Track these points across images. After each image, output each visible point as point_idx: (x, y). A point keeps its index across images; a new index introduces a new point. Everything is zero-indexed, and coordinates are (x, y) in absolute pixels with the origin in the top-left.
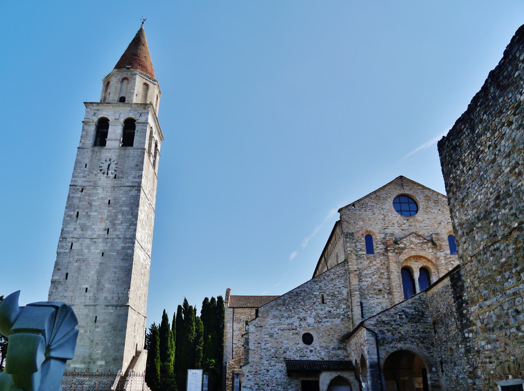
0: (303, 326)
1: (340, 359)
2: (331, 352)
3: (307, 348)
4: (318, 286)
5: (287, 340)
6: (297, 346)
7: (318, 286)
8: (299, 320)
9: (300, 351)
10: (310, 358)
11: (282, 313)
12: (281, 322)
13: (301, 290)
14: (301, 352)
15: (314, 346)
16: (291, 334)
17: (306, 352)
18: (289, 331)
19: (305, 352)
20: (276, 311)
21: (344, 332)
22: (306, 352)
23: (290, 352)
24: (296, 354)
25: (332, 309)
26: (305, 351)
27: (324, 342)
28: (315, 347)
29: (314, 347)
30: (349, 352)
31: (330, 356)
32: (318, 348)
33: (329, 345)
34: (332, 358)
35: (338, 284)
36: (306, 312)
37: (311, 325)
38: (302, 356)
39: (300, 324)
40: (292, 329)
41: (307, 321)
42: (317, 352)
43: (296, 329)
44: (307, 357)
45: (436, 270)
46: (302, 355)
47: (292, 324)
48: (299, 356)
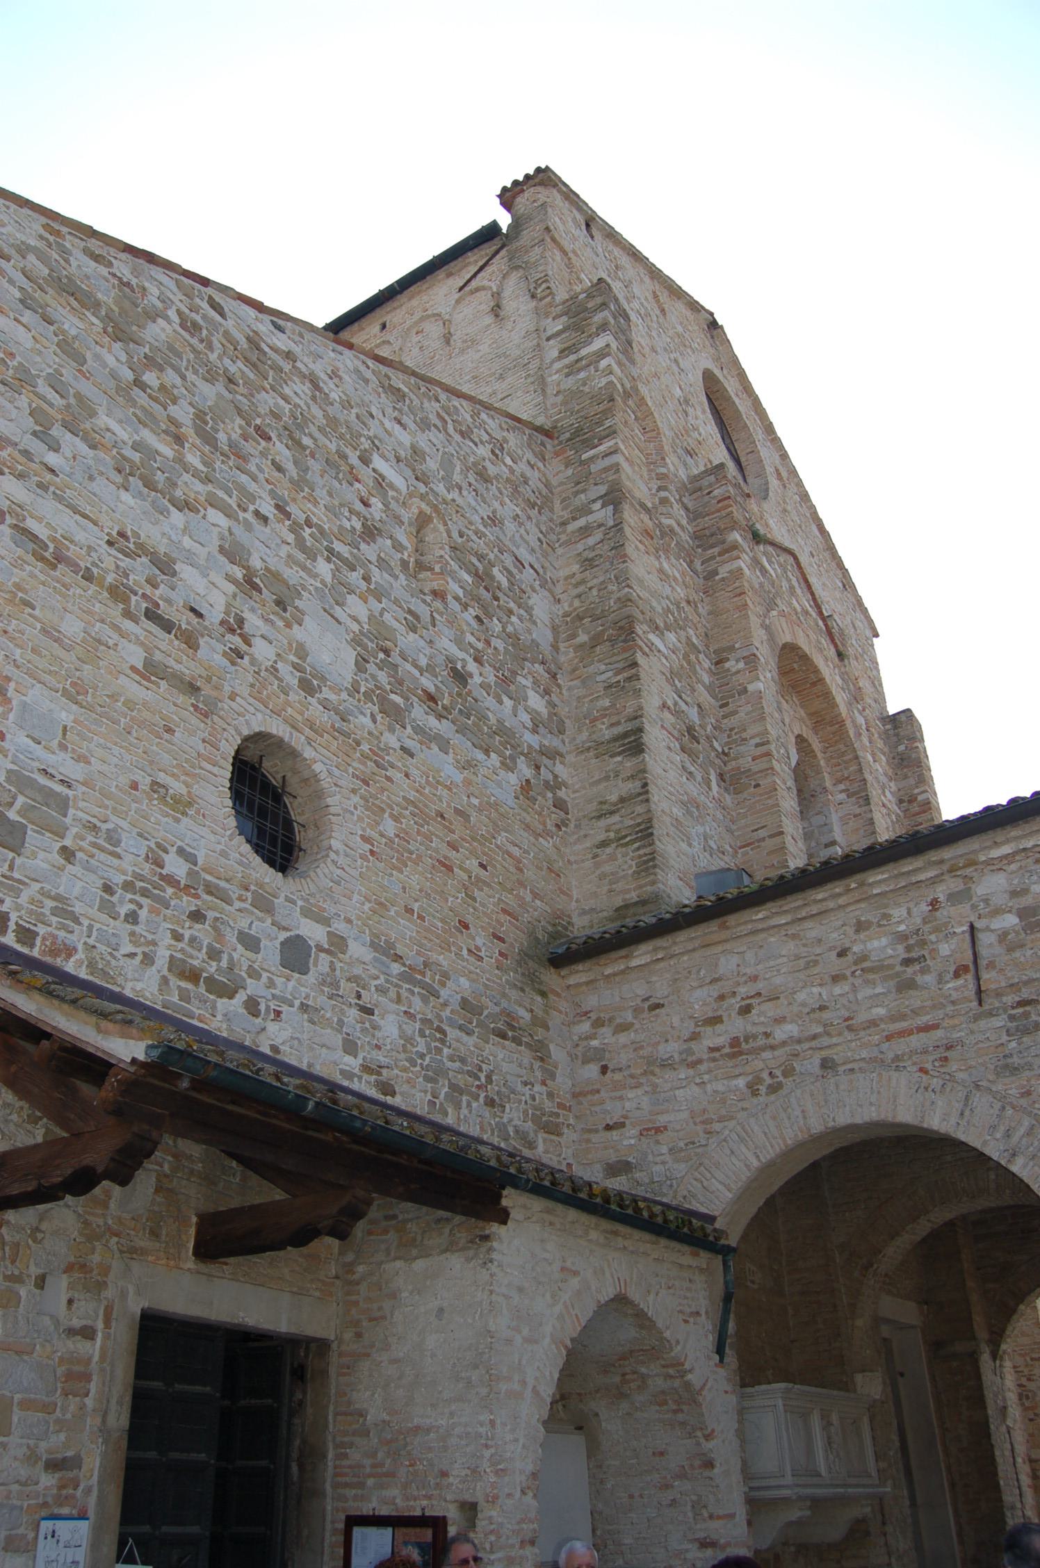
0: (263, 651)
1: (502, 1128)
2: (452, 1033)
3: (264, 904)
4: (405, 438)
5: (75, 693)
6: (162, 825)
7: (405, 438)
8: (239, 573)
9: (188, 903)
10: (272, 1027)
11: (85, 388)
12: (52, 459)
13: (289, 355)
14: (197, 916)
15: (331, 909)
16: (136, 657)
17: (251, 943)
18: (116, 611)
19: (232, 938)
20: (28, 317)
21: (536, 896)
22: (251, 943)
23: (68, 854)
24: (132, 918)
25: (472, 667)
26: (243, 924)
27: (409, 911)
28: (339, 927)
29: (325, 922)
30: (563, 1083)
31: (440, 1072)
32: (358, 950)
33: (444, 960)
34: (458, 1106)
35: (510, 526)
36: (301, 544)
37: (326, 693)
38: (193, 976)
39: (241, 621)
40: (151, 615)
41: (297, 631)
42: (346, 988)
43: (190, 641)
44: (252, 1006)
45: (842, 787)
46: (198, 959)
47: (165, 566)
48: (163, 955)
